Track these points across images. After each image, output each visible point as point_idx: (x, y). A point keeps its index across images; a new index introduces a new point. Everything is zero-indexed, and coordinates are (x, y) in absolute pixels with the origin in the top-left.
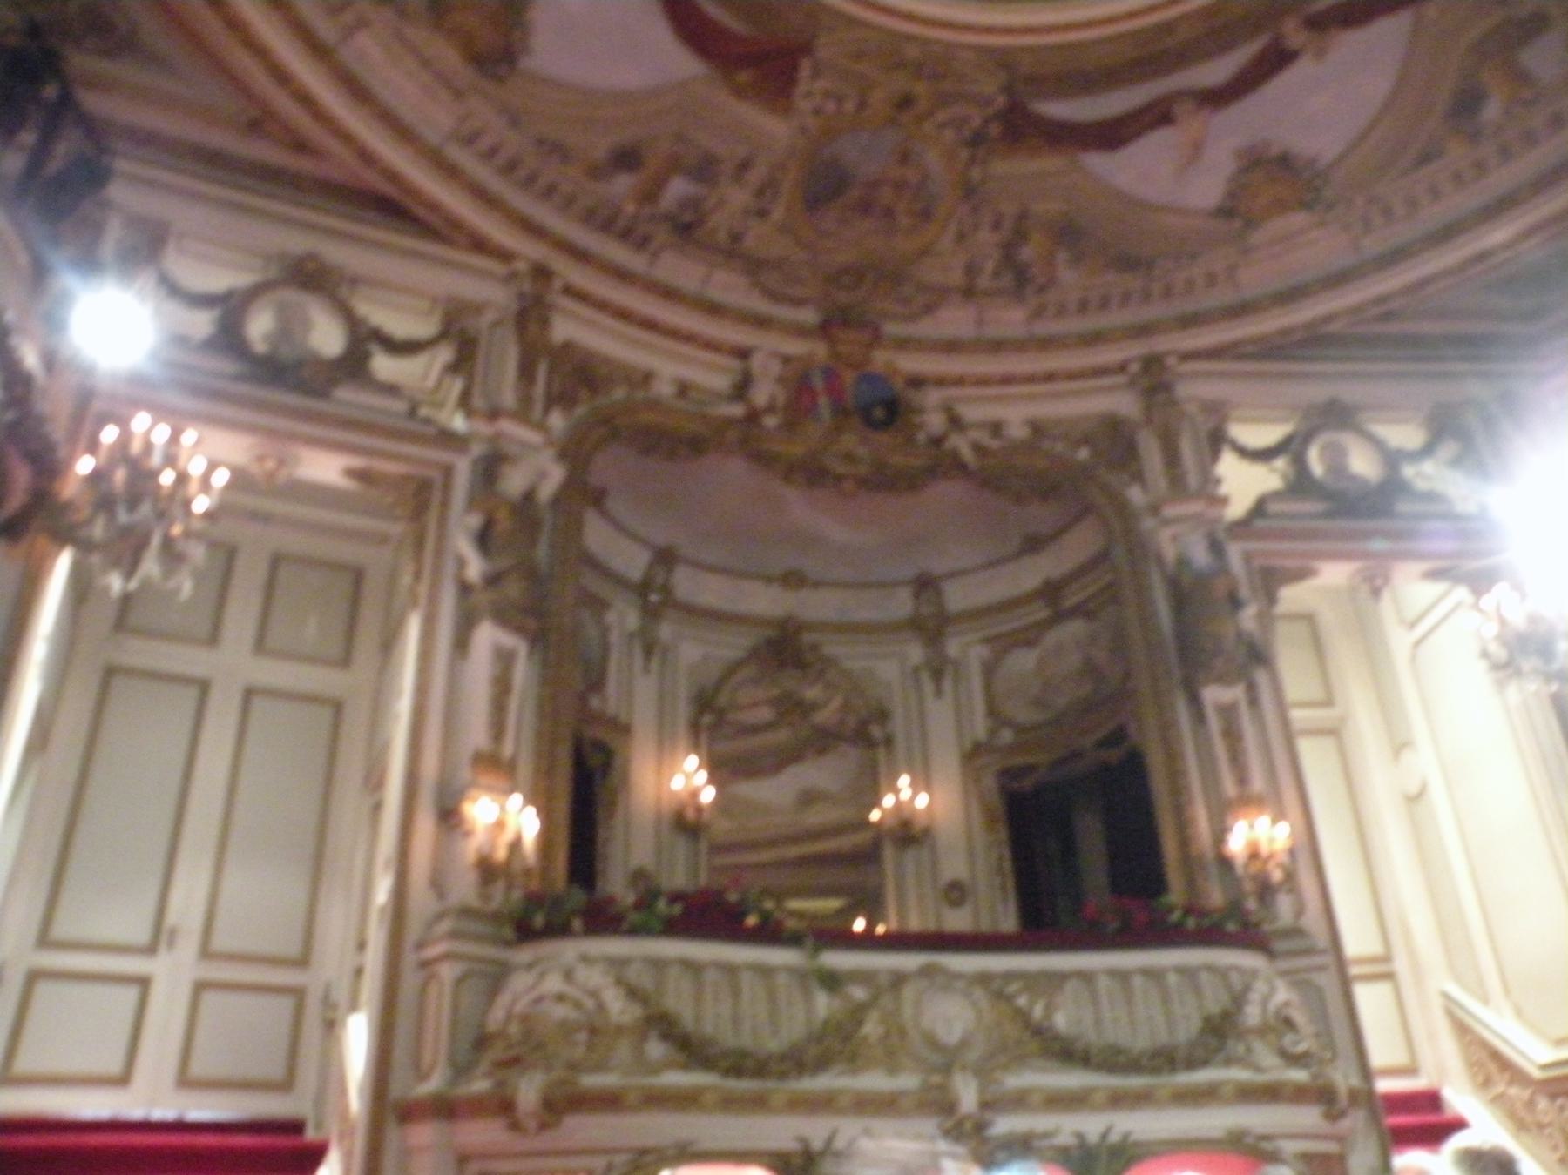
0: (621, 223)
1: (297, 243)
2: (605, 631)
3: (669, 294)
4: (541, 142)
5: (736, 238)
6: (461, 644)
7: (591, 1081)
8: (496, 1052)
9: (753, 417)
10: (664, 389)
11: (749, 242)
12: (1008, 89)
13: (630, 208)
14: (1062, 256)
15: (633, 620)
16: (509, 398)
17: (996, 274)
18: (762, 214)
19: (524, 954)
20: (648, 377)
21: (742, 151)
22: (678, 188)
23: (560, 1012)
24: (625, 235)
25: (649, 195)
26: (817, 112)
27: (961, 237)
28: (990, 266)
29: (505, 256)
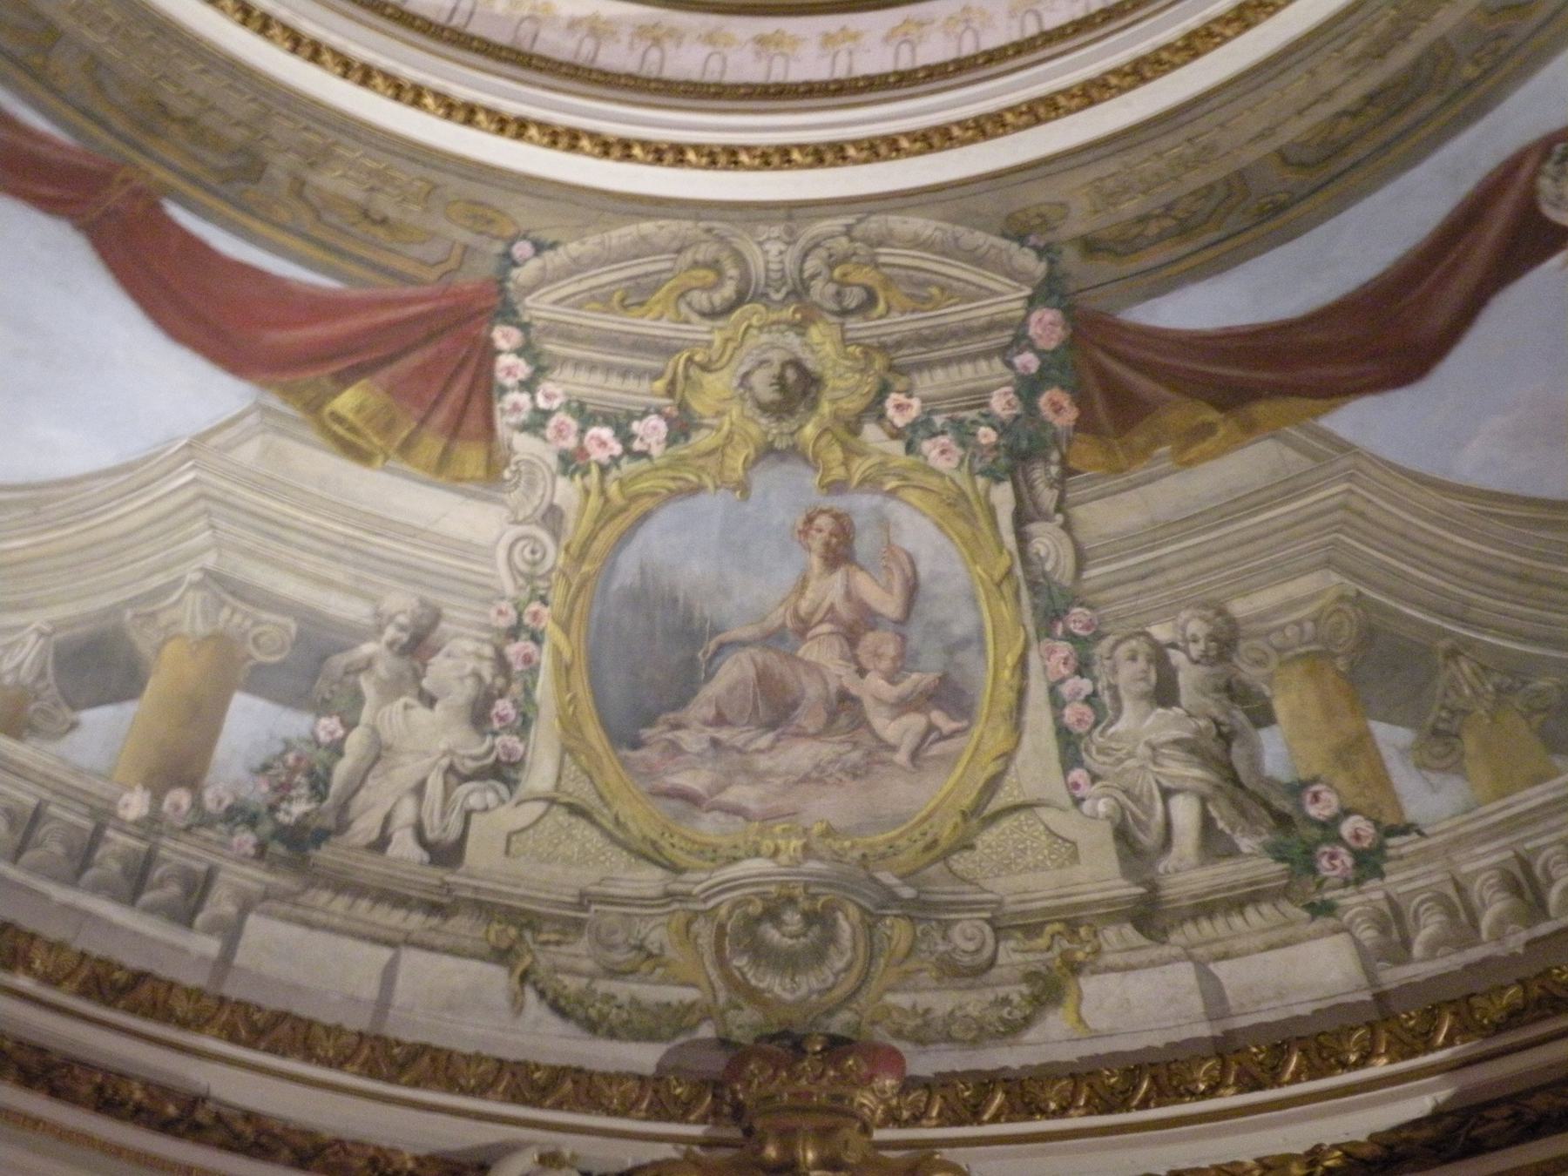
5: (447, 854)
11: (482, 855)
12: (1048, 291)
13: (135, 805)
14: (1391, 737)
17: (1213, 842)
18: (503, 772)
21: (401, 603)
26: (571, 462)
27: (1070, 746)
28: (1185, 813)
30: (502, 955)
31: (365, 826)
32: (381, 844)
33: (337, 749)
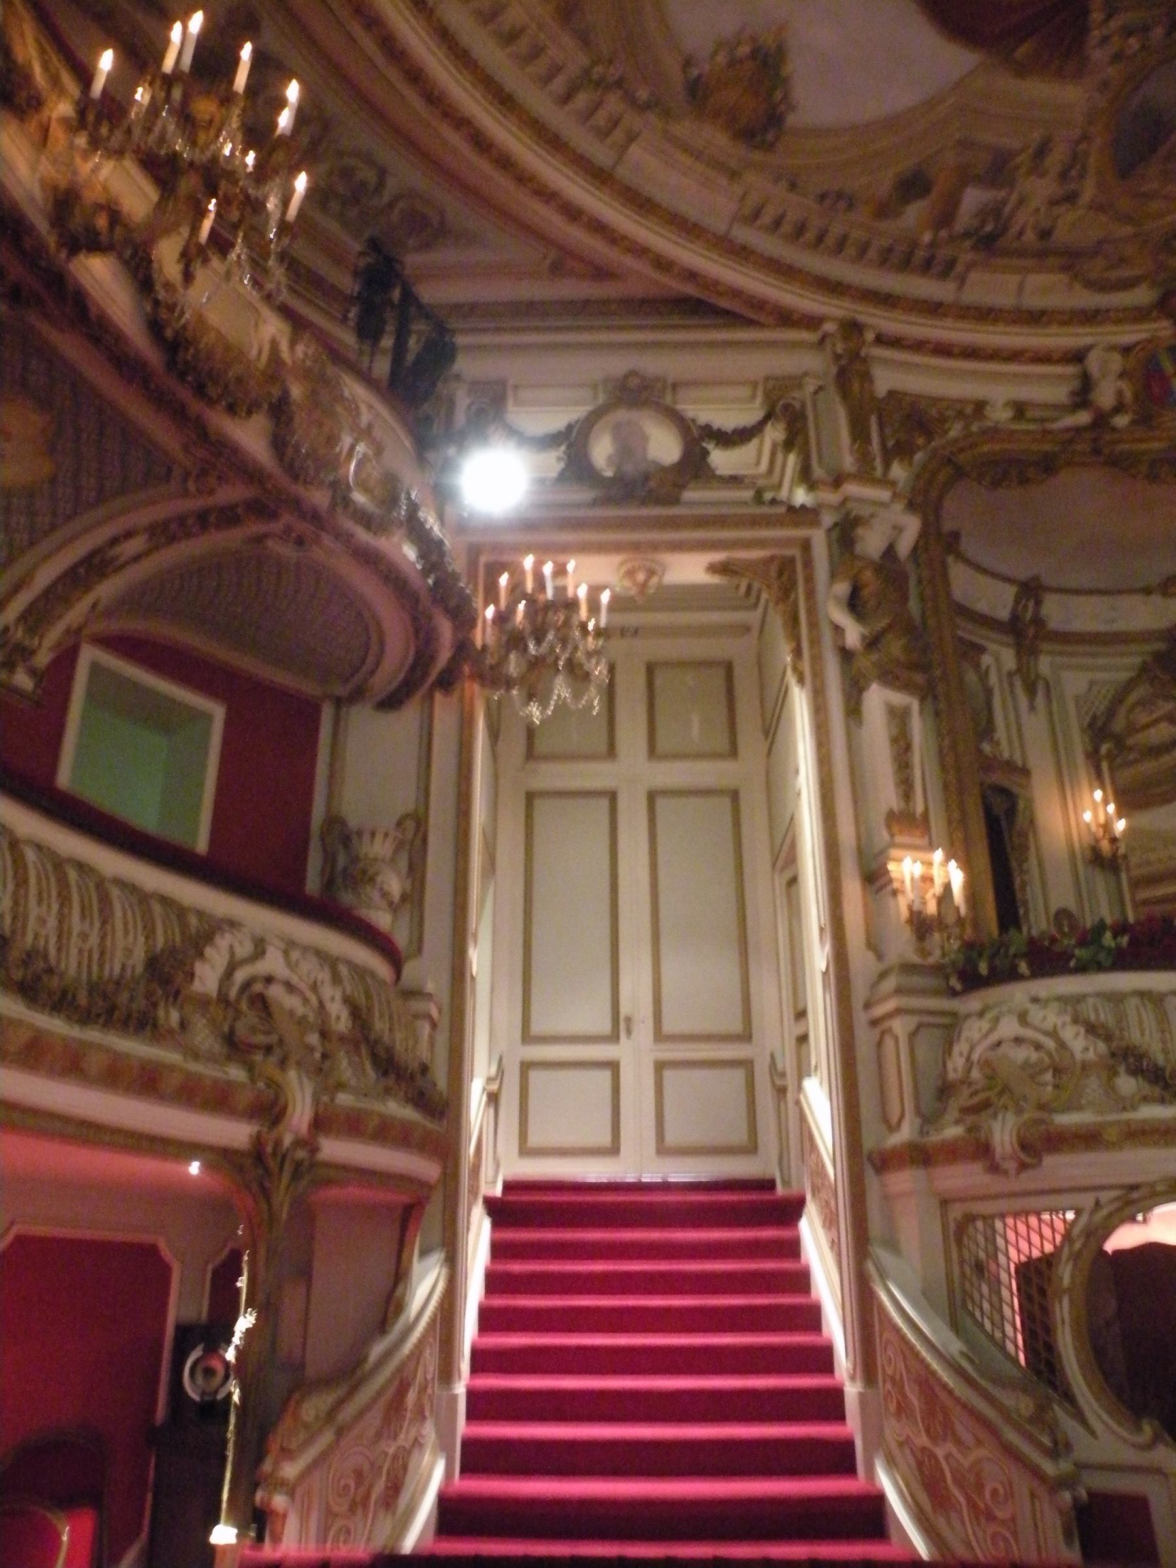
0: (921, 254)
1: (618, 365)
2: (984, 677)
3: (986, 315)
4: (822, 197)
5: (1045, 234)
6: (854, 711)
7: (1067, 1120)
8: (963, 1098)
9: (1101, 421)
10: (1000, 415)
13: (927, 237)
15: (1009, 659)
16: (848, 462)
19: (973, 1002)
20: (980, 406)
22: (973, 198)
23: (1021, 1054)
24: (926, 267)
25: (945, 218)
29: (811, 322)
30: (1065, 269)
31: (1014, 230)
32: (1021, 234)
33: (1004, 202)
